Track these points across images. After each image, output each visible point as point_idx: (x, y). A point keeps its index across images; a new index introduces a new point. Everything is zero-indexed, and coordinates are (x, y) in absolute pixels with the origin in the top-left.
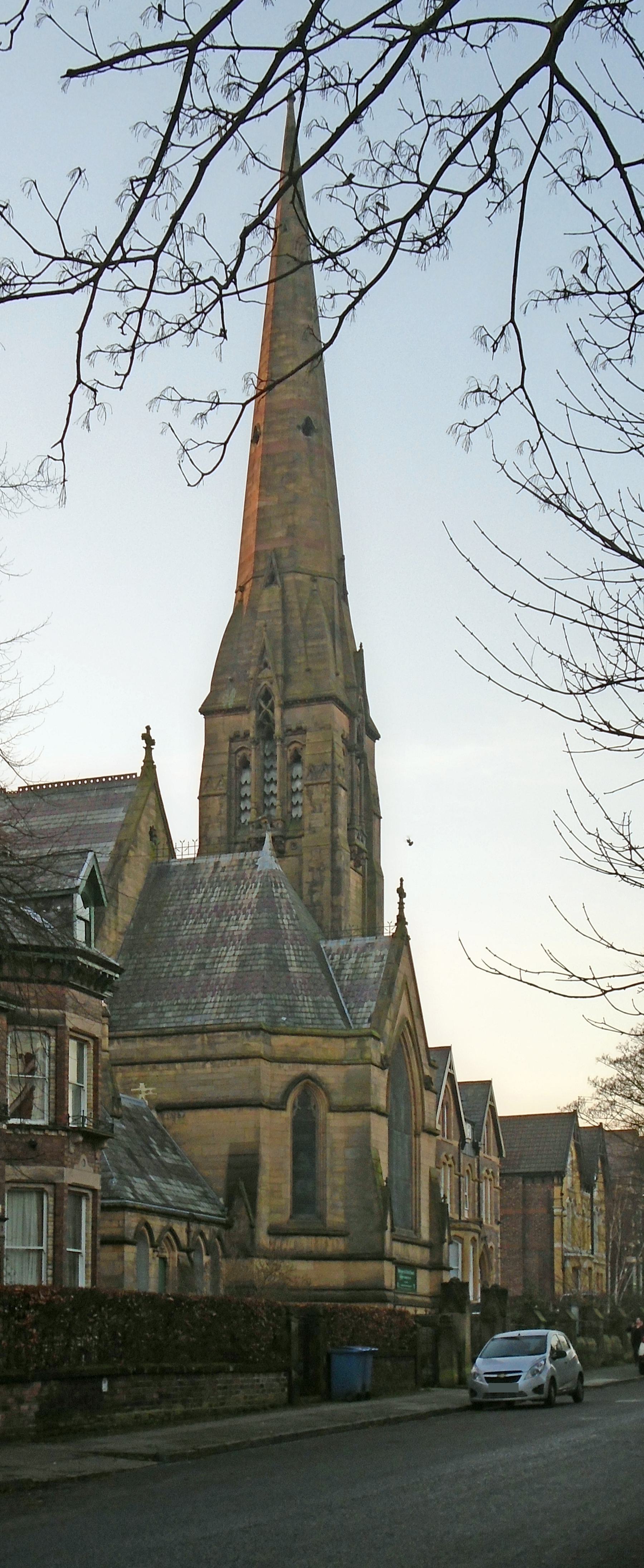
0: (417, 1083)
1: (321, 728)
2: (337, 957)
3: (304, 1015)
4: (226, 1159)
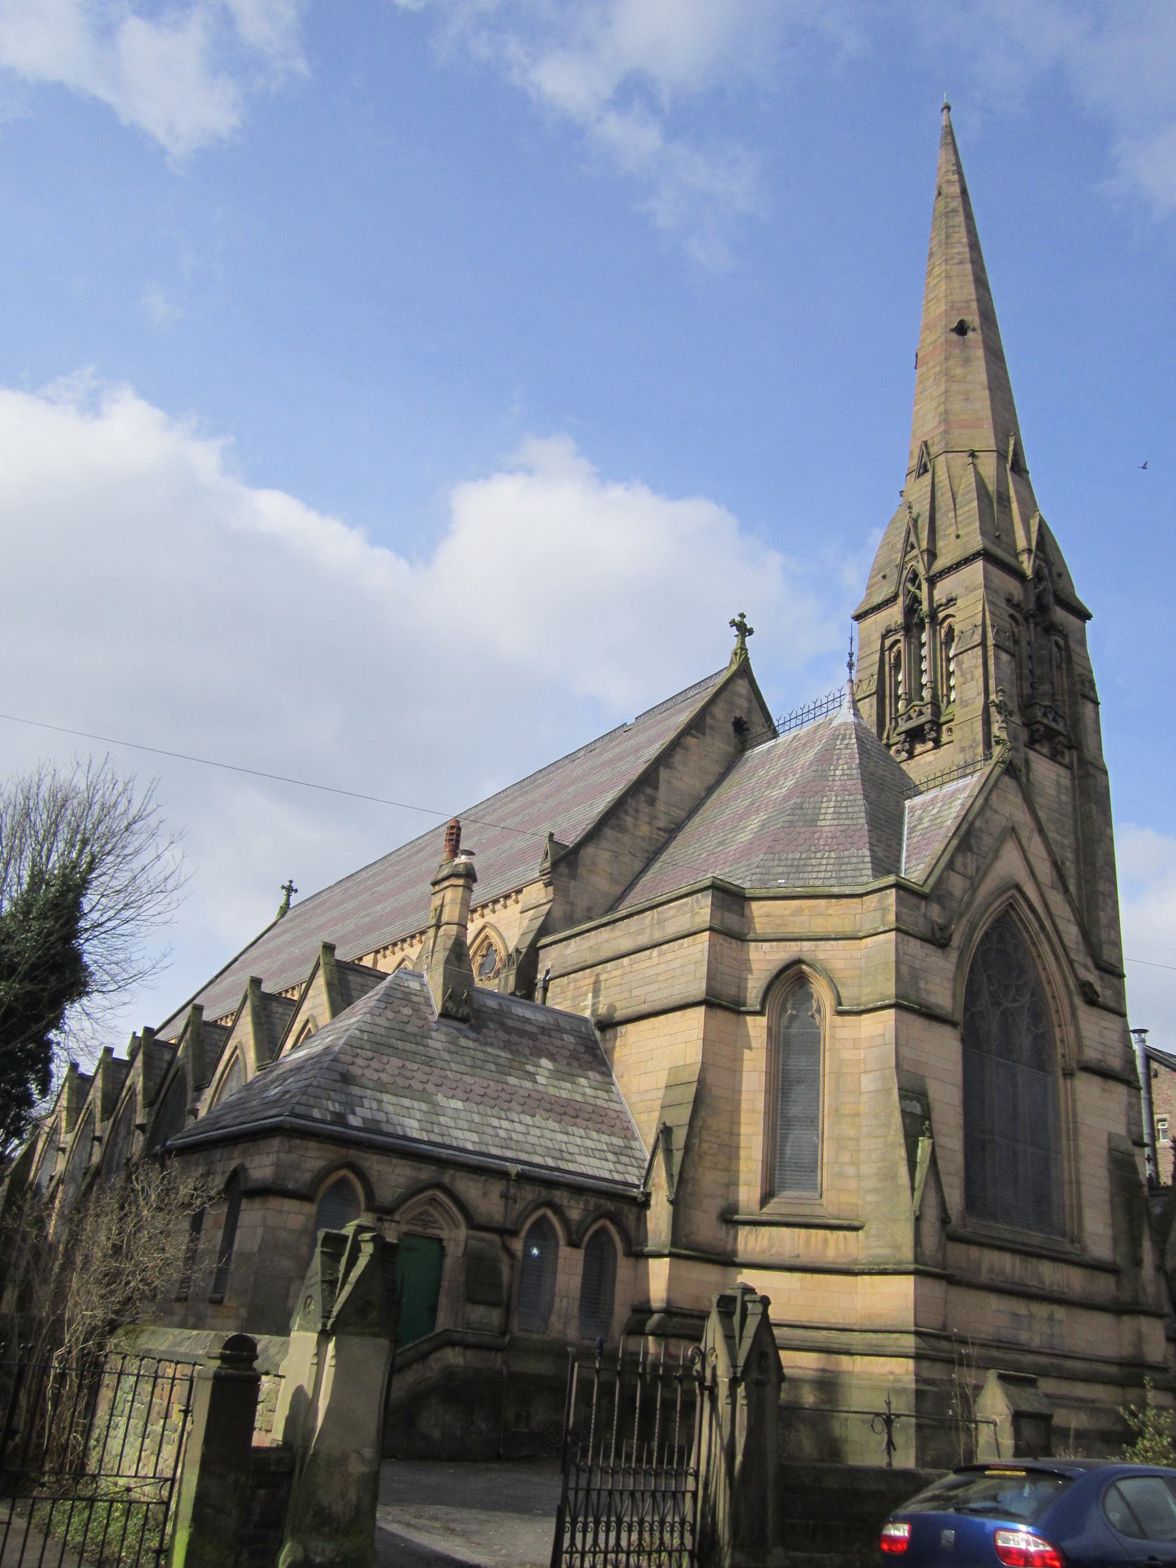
0: (1062, 991)
1: (971, 591)
2: (919, 812)
3: (814, 875)
4: (661, 1093)
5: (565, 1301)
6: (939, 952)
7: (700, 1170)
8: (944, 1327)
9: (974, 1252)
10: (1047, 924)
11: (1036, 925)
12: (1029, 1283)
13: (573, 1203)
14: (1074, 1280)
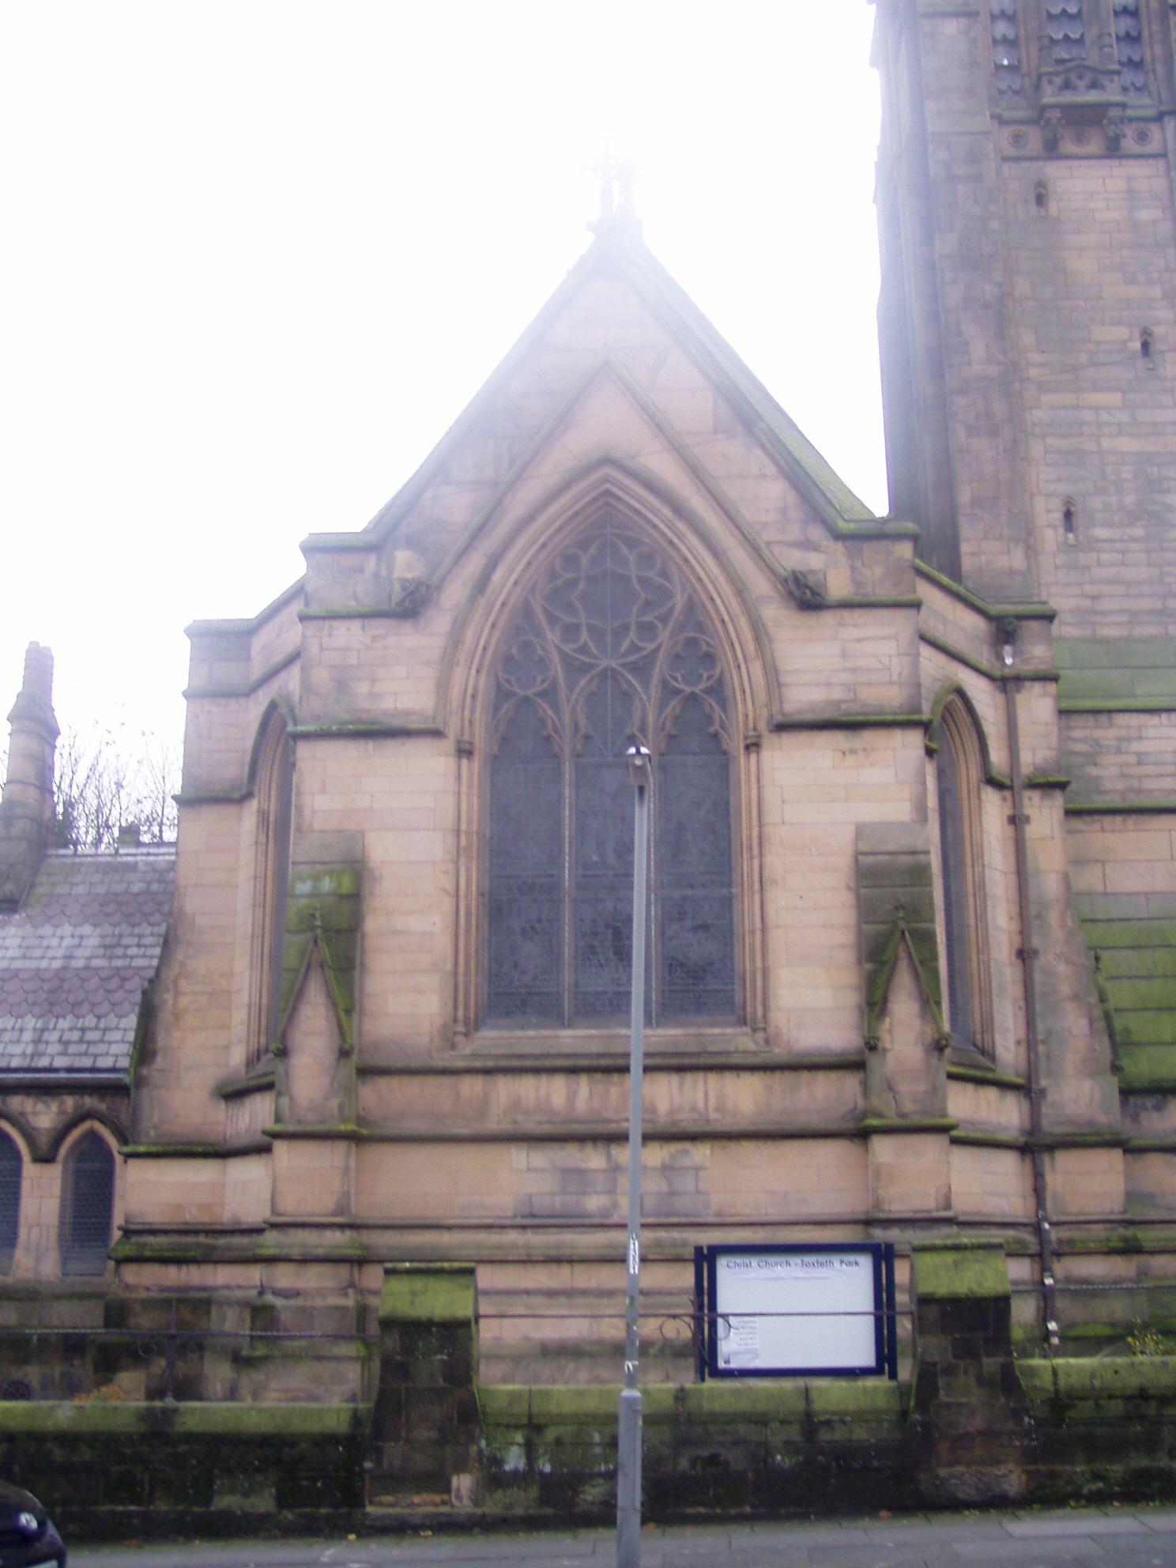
5: (35, 1232)
6: (407, 626)
7: (177, 1034)
8: (340, 1210)
9: (471, 1086)
10: (698, 504)
11: (666, 511)
12: (610, 1115)
13: (40, 1107)
14: (744, 1098)
